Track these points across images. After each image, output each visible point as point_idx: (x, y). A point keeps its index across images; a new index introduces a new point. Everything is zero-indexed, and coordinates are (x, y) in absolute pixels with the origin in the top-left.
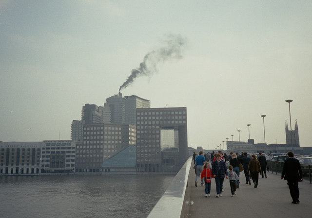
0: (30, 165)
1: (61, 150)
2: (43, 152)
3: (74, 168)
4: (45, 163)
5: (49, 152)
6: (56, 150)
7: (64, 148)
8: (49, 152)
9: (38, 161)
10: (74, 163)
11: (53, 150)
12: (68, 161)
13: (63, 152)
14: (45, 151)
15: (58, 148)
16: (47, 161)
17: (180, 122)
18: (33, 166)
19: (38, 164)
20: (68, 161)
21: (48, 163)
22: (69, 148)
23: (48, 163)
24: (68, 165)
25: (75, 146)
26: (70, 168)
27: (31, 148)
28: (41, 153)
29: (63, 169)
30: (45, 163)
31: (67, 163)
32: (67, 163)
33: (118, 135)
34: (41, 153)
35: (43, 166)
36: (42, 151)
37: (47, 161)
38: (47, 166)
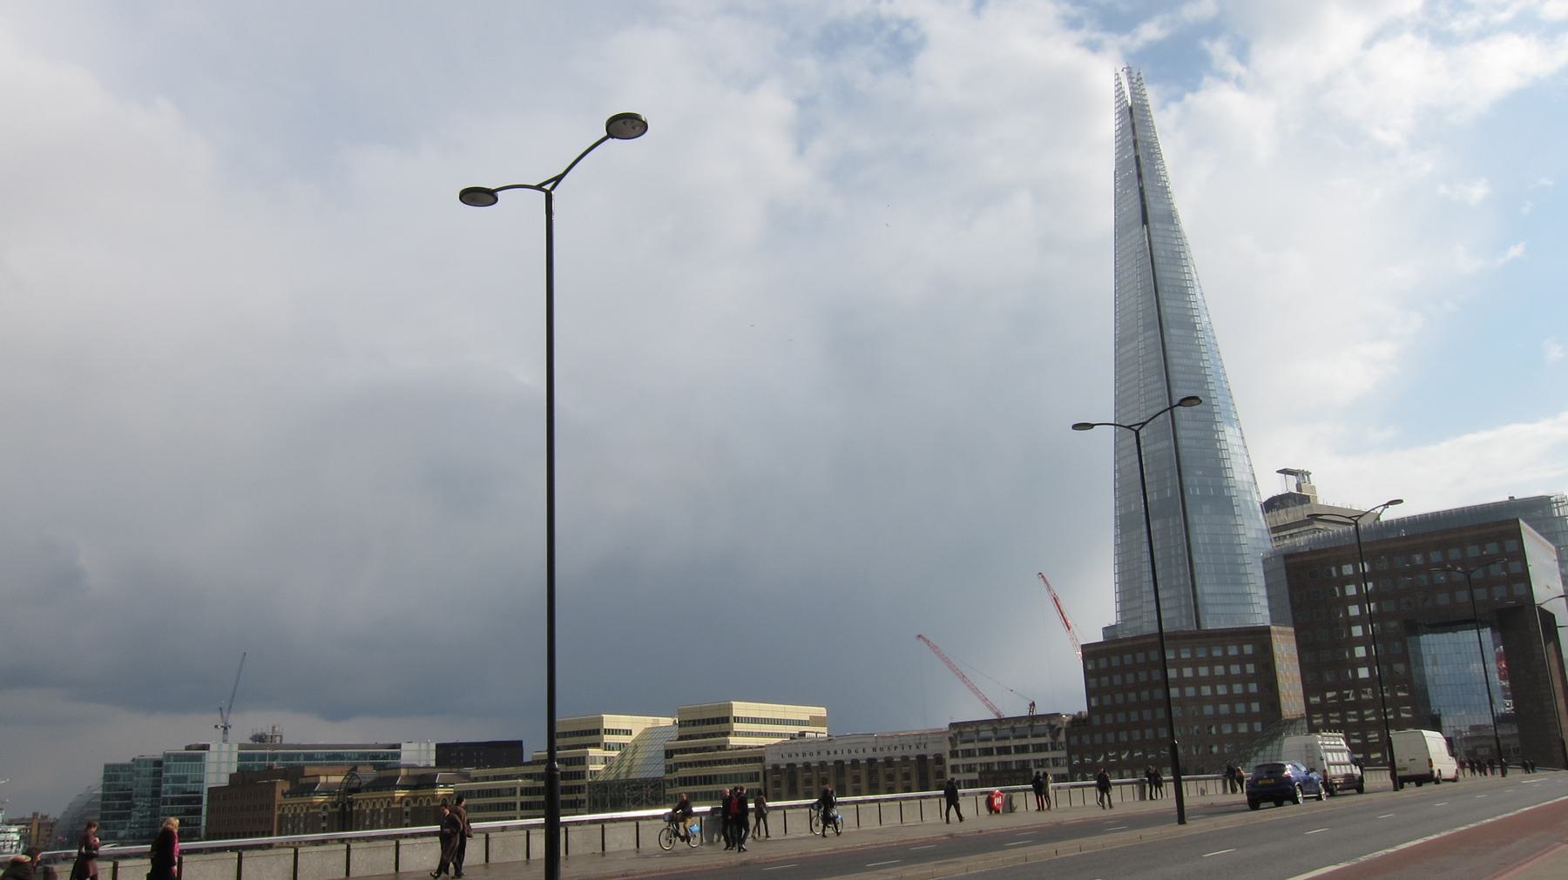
1: (1014, 757)
2: (954, 769)
5: (970, 769)
6: (995, 759)
7: (1022, 749)
8: (970, 769)
11: (987, 759)
13: (1025, 763)
14: (959, 761)
15: (1004, 750)
22: (1040, 748)
25: (1062, 738)
27: (913, 753)
28: (948, 770)
33: (1228, 679)
34: (948, 770)
36: (950, 762)
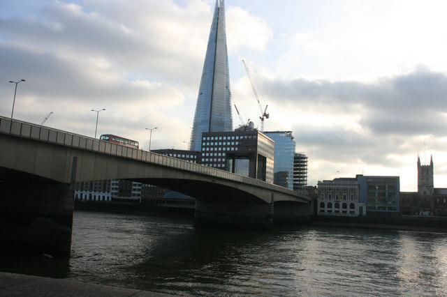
3: (140, 197)
4: (114, 191)
9: (109, 188)
10: (140, 193)
12: (135, 190)
16: (116, 189)
18: (104, 194)
19: (108, 192)
20: (135, 190)
21: (117, 191)
23: (117, 191)
24: (134, 195)
26: (136, 198)
29: (130, 198)
30: (114, 191)
31: (133, 192)
32: (133, 192)
35: (112, 193)
37: (116, 189)
38: (116, 194)
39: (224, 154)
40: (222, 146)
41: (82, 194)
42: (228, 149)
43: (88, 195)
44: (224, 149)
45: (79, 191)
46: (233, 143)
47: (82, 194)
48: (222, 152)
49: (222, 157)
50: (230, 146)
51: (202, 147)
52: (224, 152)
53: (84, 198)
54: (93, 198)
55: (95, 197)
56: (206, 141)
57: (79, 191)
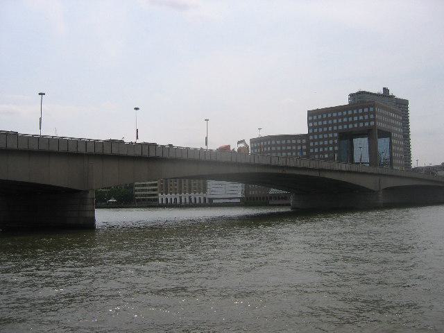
0: (202, 193)
17: (367, 124)
39: (336, 135)
40: (333, 125)
41: (181, 198)
42: (340, 127)
43: (187, 199)
44: (335, 128)
45: (178, 194)
46: (366, 117)
47: (181, 198)
48: (333, 131)
49: (333, 138)
50: (343, 123)
51: (309, 128)
52: (336, 131)
53: (183, 201)
54: (193, 201)
55: (195, 199)
56: (369, 120)
57: (178, 194)
